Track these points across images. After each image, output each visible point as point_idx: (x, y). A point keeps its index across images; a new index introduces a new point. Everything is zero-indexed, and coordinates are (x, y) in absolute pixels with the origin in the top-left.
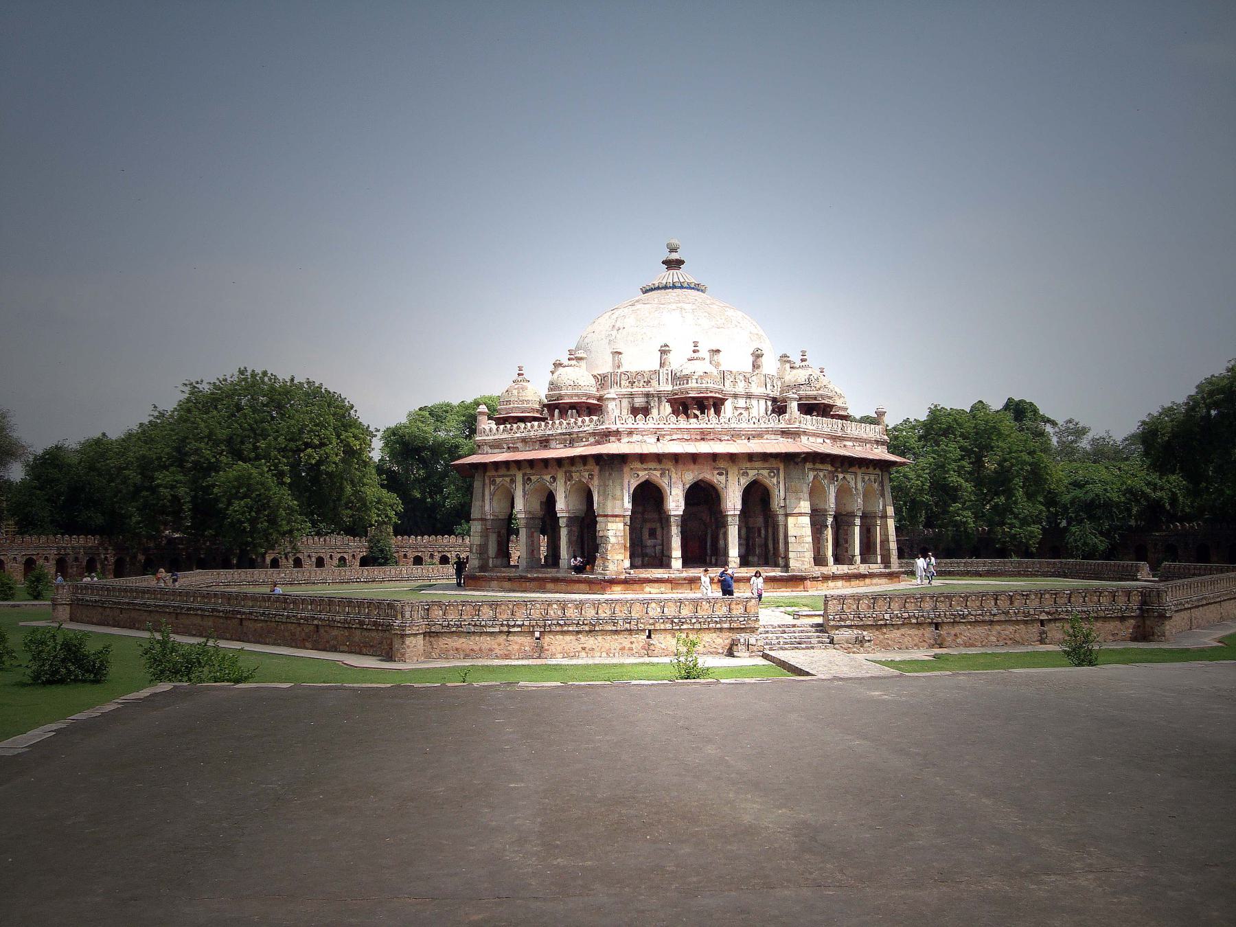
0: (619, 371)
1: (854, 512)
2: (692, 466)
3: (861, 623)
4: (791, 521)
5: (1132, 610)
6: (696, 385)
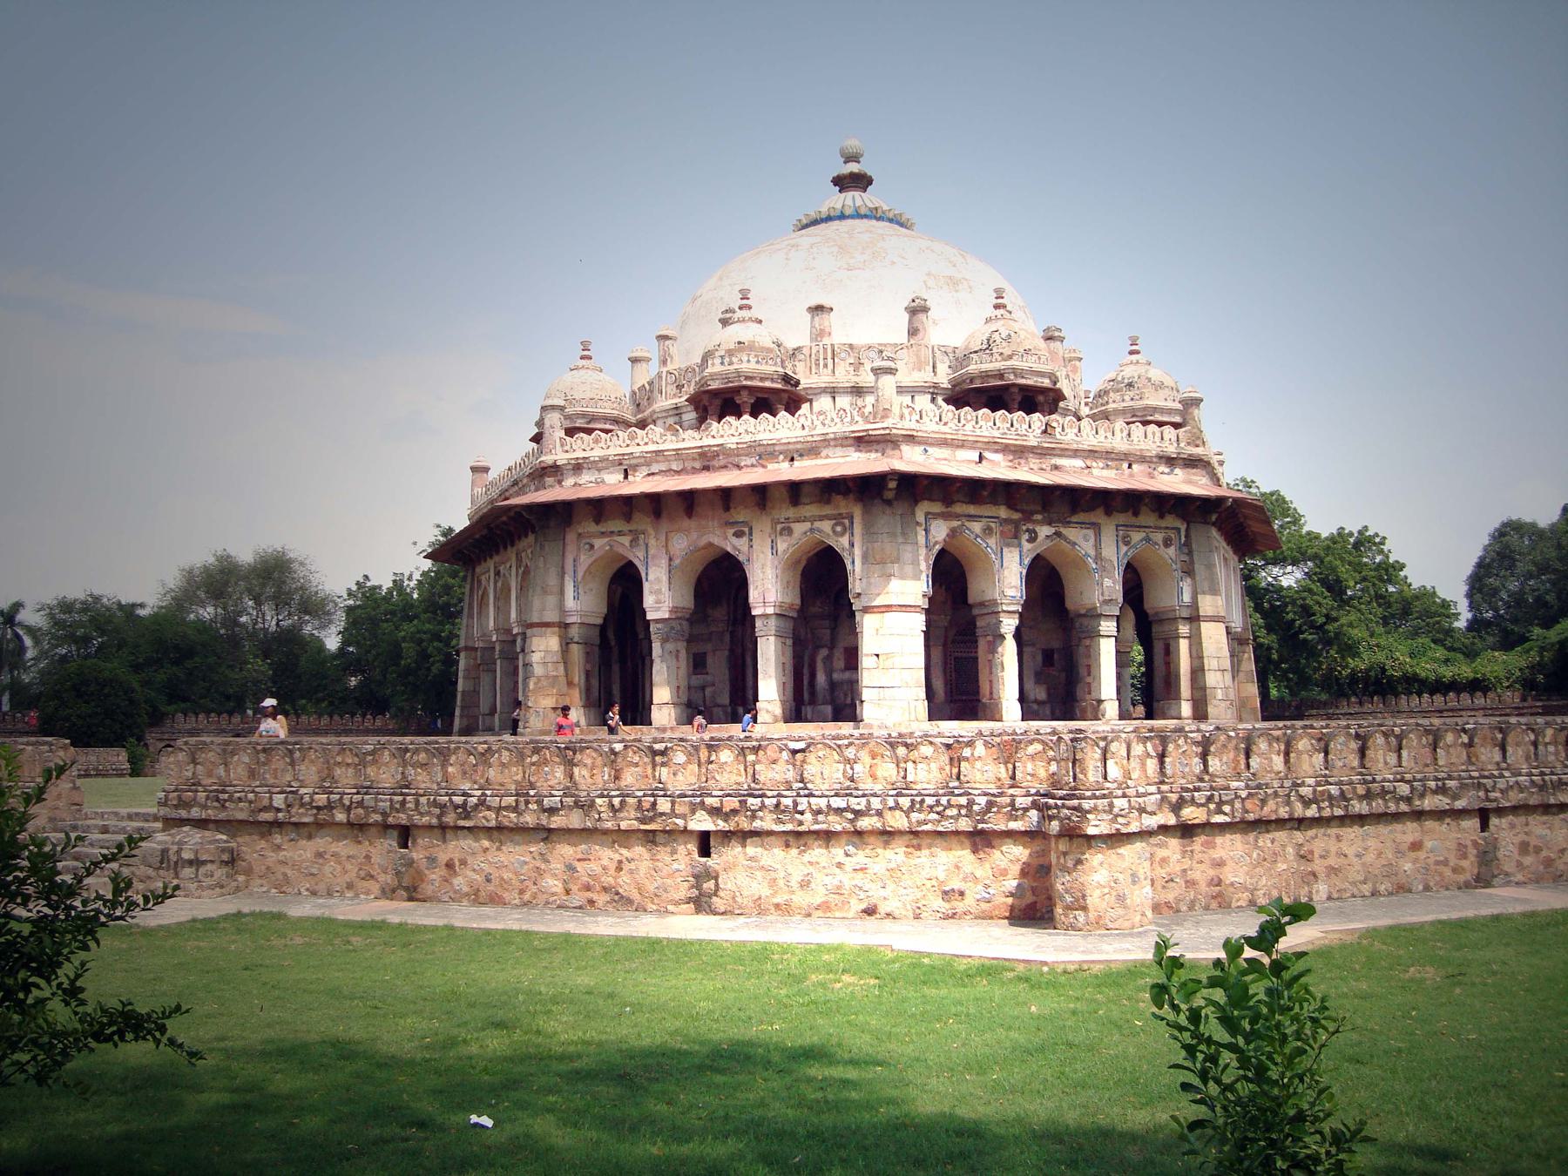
0: (665, 370)
1: (1096, 608)
2: (686, 523)
3: (222, 816)
4: (869, 626)
5: (1014, 812)
6: (723, 368)
